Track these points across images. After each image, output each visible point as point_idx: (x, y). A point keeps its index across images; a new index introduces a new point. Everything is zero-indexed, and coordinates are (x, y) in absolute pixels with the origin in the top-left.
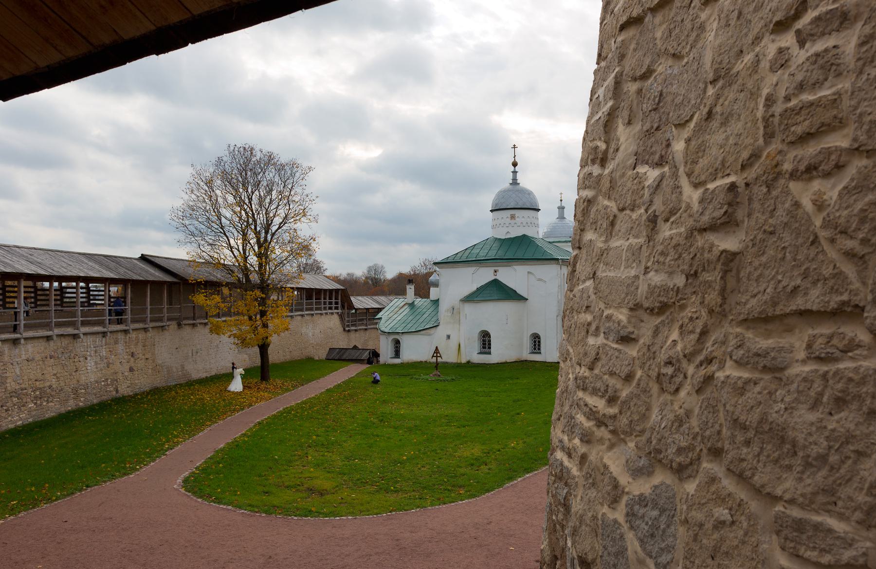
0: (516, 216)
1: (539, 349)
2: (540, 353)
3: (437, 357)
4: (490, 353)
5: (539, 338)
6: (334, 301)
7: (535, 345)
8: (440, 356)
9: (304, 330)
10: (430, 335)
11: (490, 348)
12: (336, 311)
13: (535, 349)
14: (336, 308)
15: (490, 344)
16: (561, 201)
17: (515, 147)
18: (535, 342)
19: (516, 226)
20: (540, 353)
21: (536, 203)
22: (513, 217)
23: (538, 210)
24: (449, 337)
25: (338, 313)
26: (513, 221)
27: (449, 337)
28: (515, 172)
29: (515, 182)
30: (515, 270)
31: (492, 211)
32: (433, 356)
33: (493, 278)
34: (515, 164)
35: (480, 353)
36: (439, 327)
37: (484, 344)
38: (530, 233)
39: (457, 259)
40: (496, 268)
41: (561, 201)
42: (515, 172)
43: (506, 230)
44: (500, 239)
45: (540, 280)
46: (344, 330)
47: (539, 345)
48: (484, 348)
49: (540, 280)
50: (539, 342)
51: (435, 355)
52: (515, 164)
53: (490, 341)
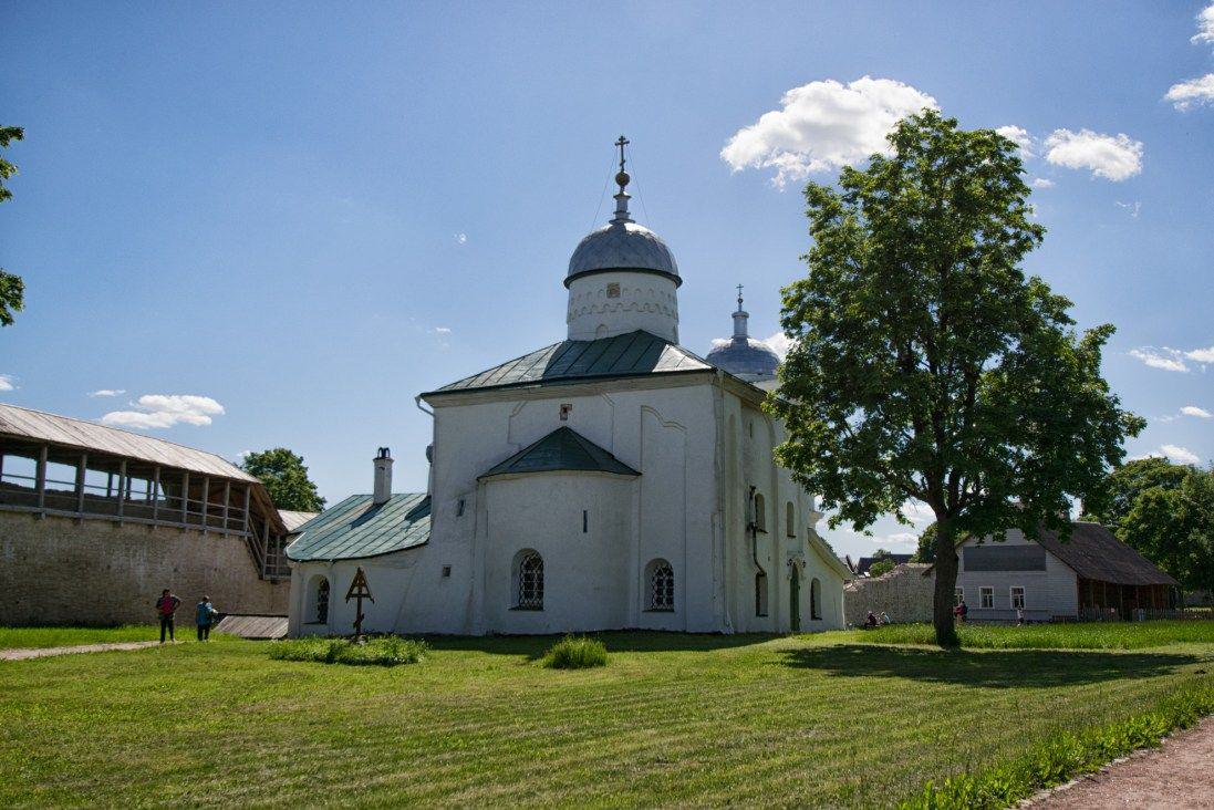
0: (622, 287)
1: (670, 601)
2: (672, 611)
3: (360, 596)
4: (540, 608)
5: (671, 574)
6: (226, 506)
7: (659, 592)
8: (368, 596)
9: (118, 560)
11: (541, 595)
12: (240, 533)
13: (659, 601)
14: (240, 527)
15: (541, 586)
16: (740, 301)
17: (622, 142)
18: (660, 583)
20: (672, 611)
22: (613, 291)
23: (678, 281)
24: (447, 572)
25: (241, 537)
26: (612, 302)
27: (447, 572)
31: (567, 283)
32: (350, 595)
33: (555, 423)
34: (623, 180)
35: (519, 608)
37: (529, 586)
40: (566, 401)
41: (740, 301)
42: (621, 198)
44: (583, 342)
45: (669, 424)
46: (261, 578)
47: (670, 592)
48: (528, 595)
49: (669, 424)
50: (670, 583)
51: (356, 591)
52: (623, 180)
53: (541, 578)
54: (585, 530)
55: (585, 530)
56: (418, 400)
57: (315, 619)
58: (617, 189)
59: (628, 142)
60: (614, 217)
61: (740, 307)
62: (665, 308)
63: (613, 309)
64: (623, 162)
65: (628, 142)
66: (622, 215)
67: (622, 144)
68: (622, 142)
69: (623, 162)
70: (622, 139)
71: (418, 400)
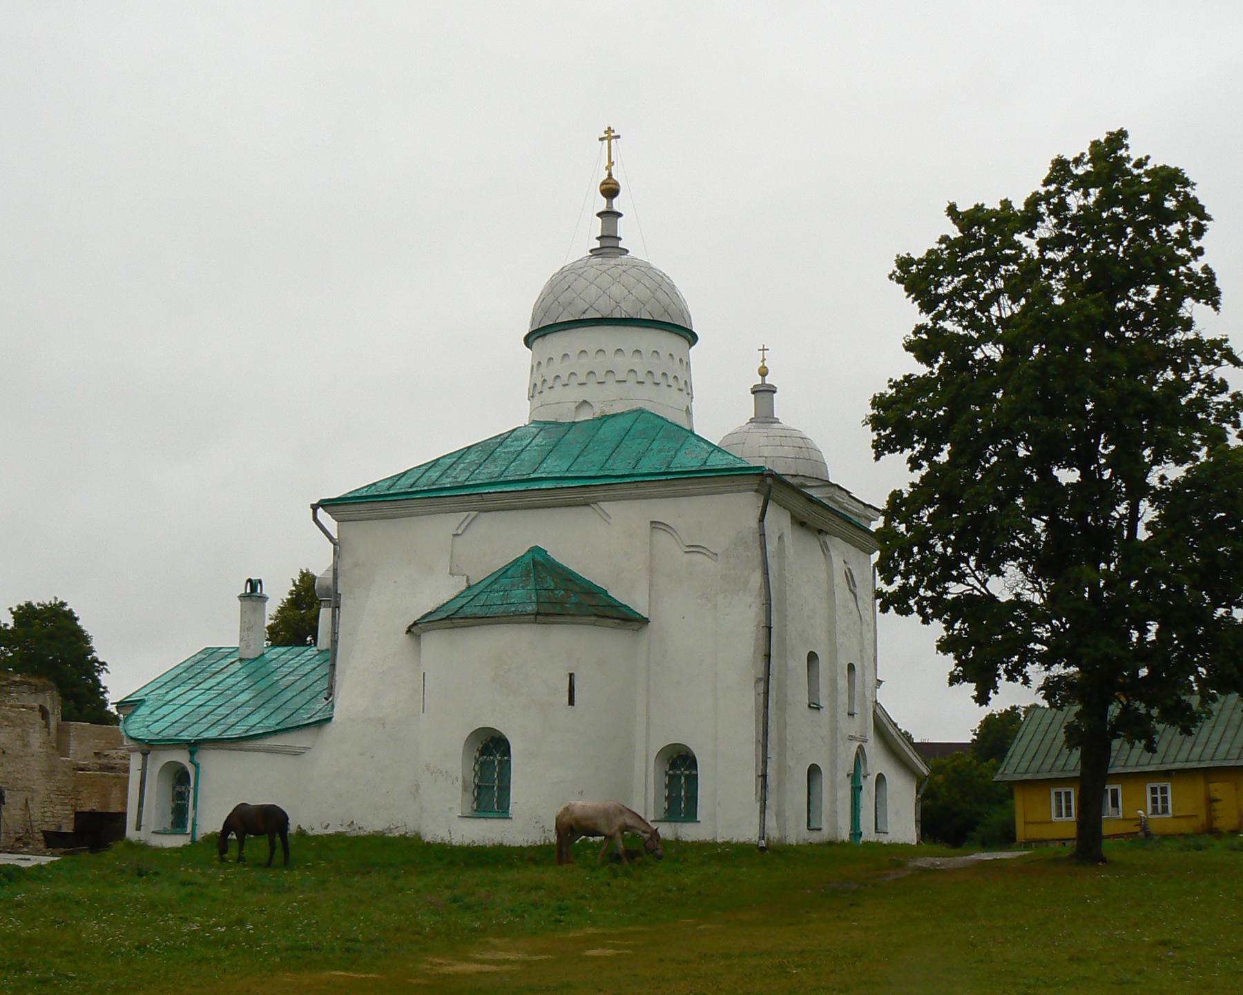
10: (295, 753)
17: (610, 136)
19: (610, 380)
21: (683, 313)
23: (692, 338)
28: (609, 216)
29: (609, 245)
30: (606, 517)
31: (528, 341)
34: (610, 191)
36: (329, 729)
38: (663, 404)
39: (403, 485)
42: (609, 216)
43: (577, 394)
44: (556, 424)
45: (694, 549)
52: (610, 191)
54: (571, 702)
55: (571, 702)
56: (315, 508)
57: (168, 826)
58: (602, 204)
59: (618, 137)
60: (597, 244)
61: (763, 380)
62: (675, 377)
63: (600, 379)
64: (611, 163)
65: (618, 137)
66: (609, 245)
67: (609, 139)
68: (610, 136)
69: (611, 163)
70: (609, 128)
71: (315, 508)
